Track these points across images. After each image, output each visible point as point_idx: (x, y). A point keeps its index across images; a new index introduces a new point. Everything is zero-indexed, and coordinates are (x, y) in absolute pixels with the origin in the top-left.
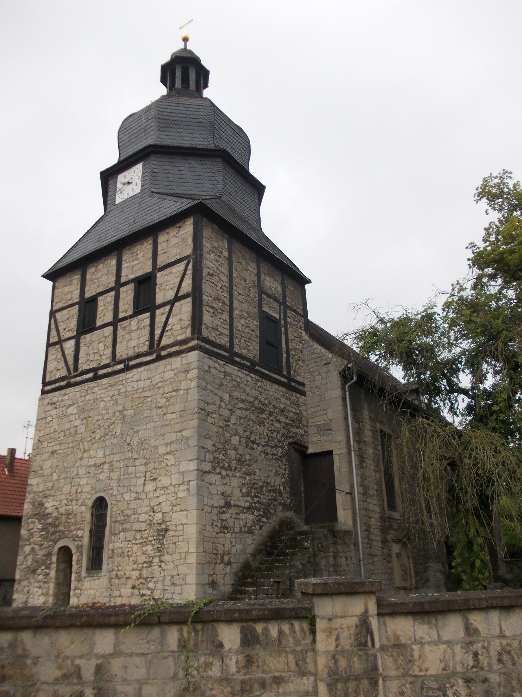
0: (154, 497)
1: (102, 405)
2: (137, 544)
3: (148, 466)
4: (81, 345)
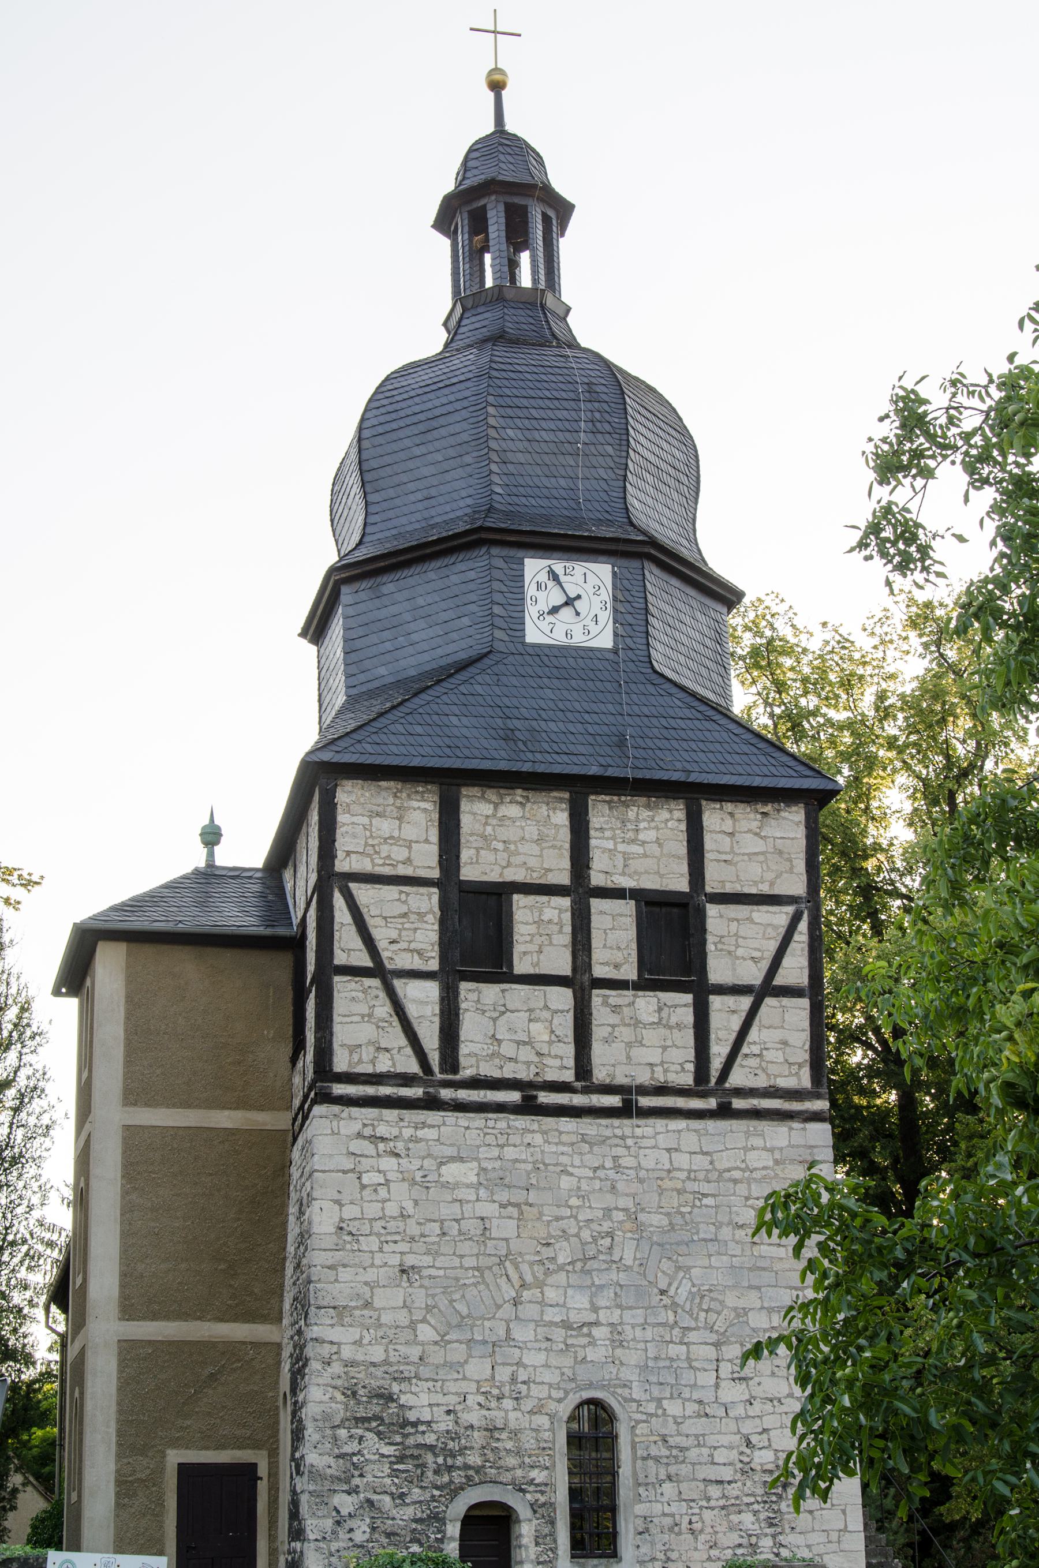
0: (748, 1417)
1: (566, 1182)
2: (712, 1508)
3: (723, 1348)
4: (463, 1006)
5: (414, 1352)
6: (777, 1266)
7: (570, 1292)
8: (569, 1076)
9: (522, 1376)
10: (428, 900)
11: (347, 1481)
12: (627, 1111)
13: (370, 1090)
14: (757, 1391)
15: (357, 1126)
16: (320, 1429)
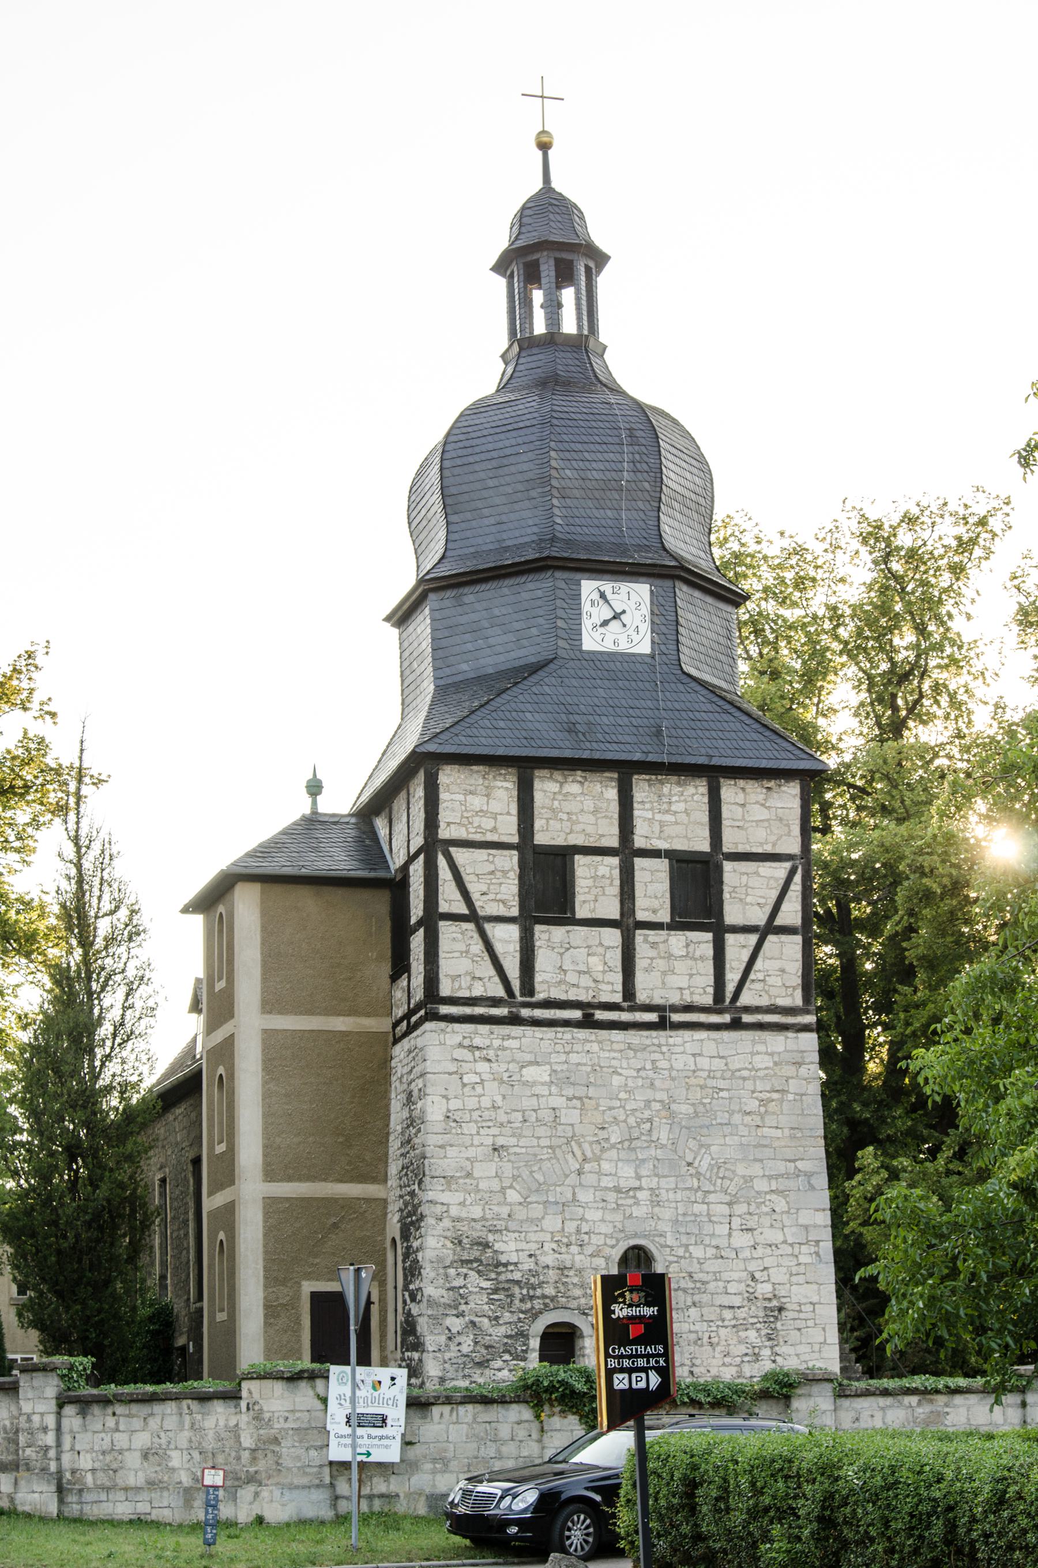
1: (616, 1081)
4: (537, 944)
5: (505, 1211)
6: (776, 1144)
7: (620, 1164)
8: (618, 998)
9: (585, 1228)
10: (510, 860)
11: (456, 1307)
12: (662, 1024)
13: (468, 1010)
14: (760, 1239)
15: (458, 1039)
16: (436, 1269)
